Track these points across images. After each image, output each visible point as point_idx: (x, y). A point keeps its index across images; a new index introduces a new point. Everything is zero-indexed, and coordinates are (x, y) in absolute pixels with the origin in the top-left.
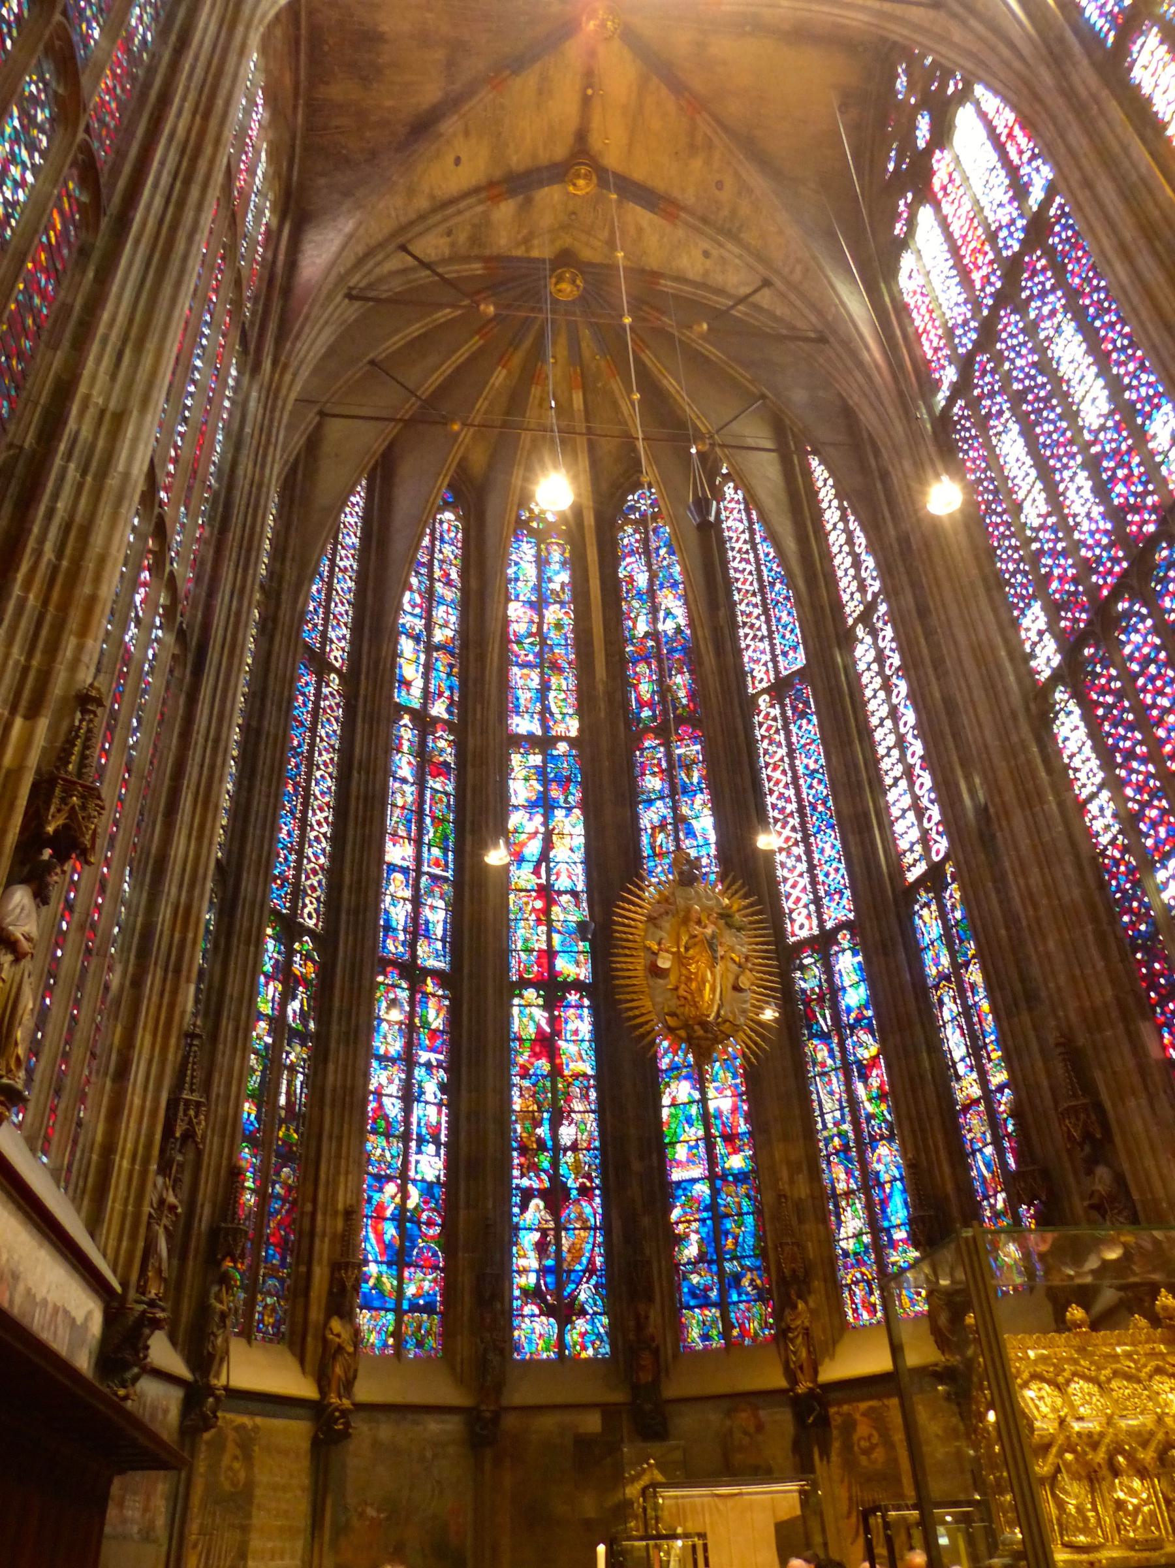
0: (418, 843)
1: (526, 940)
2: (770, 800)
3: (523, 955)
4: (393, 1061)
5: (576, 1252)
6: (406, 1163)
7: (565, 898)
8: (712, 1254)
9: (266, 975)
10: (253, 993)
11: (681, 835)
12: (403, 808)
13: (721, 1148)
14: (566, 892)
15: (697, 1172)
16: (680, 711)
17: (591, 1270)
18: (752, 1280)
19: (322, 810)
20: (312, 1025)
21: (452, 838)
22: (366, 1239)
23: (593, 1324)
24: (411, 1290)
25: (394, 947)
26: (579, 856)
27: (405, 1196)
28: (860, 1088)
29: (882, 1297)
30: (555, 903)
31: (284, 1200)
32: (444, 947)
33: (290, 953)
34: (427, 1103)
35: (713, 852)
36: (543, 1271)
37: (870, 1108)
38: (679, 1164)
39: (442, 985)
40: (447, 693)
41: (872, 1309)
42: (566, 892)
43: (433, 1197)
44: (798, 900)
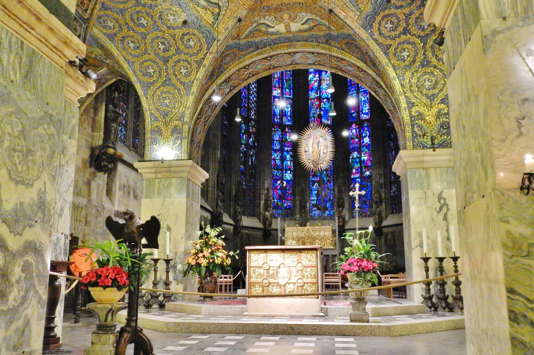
0: (282, 88)
6: (283, 176)
7: (325, 100)
10: (241, 138)
12: (277, 78)
13: (364, 170)
14: (325, 98)
18: (369, 203)
20: (256, 144)
21: (292, 85)
23: (330, 212)
27: (283, 184)
29: (398, 207)
32: (290, 118)
34: (287, 161)
41: (396, 210)
42: (325, 98)
43: (290, 183)
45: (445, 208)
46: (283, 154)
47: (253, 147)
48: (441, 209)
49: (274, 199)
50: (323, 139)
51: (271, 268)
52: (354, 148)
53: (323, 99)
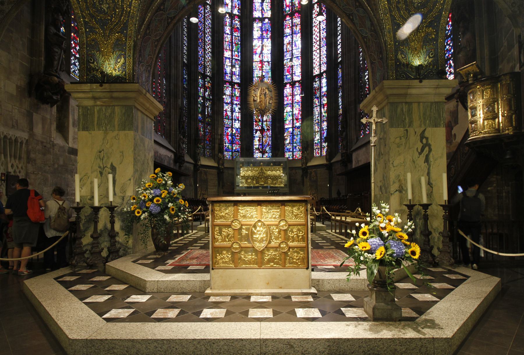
0: (232, 51)
1: (257, 74)
2: (314, 36)
3: (256, 78)
4: (229, 104)
5: (266, 141)
6: (232, 125)
8: (292, 142)
9: (200, 87)
10: (198, 91)
11: (293, 46)
12: (228, 42)
13: (295, 121)
15: (290, 126)
16: (296, 8)
17: (268, 145)
19: (208, 45)
21: (240, 49)
22: (225, 139)
24: (234, 148)
25: (228, 78)
26: (270, 52)
27: (232, 131)
28: (322, 109)
30: (264, 65)
31: (209, 133)
33: (205, 82)
35: (300, 51)
36: (259, 145)
37: (324, 114)
38: (287, 124)
39: (239, 86)
40: (238, 6)
42: (266, 62)
44: (317, 64)
45: (427, 149)
46: (232, 106)
47: (209, 100)
48: (422, 150)
49: (226, 143)
50: (269, 91)
51: (244, 227)
52: (288, 104)
53: (265, 62)
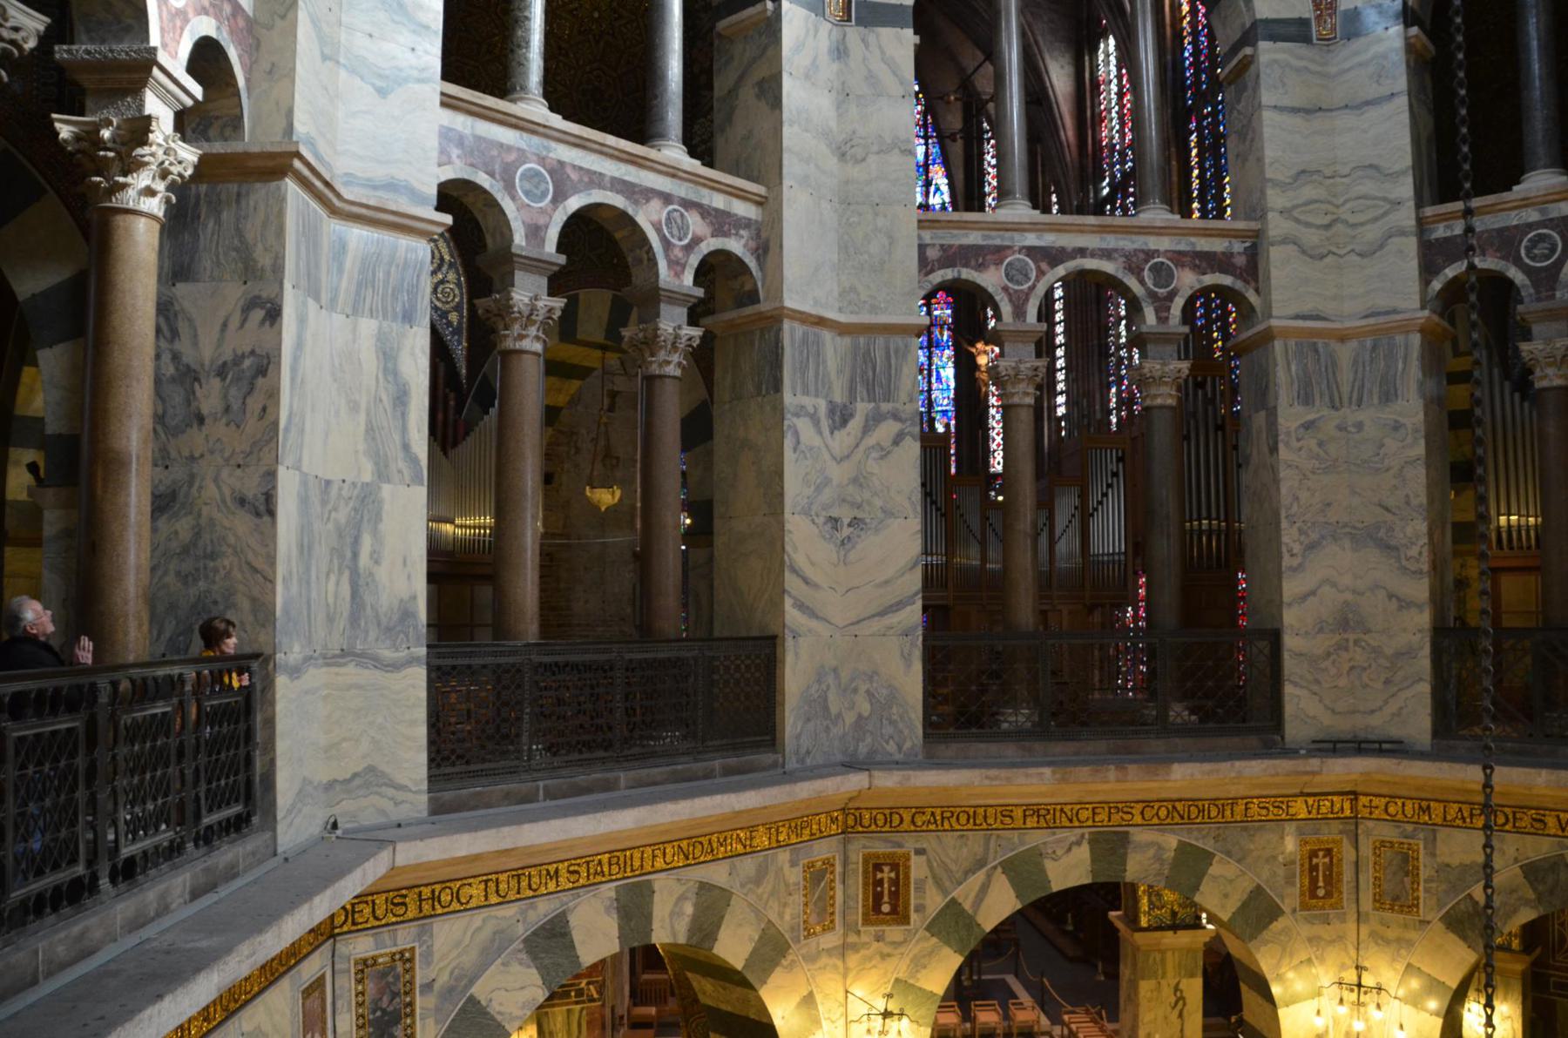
11: (933, 380)
35: (952, 396)
45: (1181, 1003)
